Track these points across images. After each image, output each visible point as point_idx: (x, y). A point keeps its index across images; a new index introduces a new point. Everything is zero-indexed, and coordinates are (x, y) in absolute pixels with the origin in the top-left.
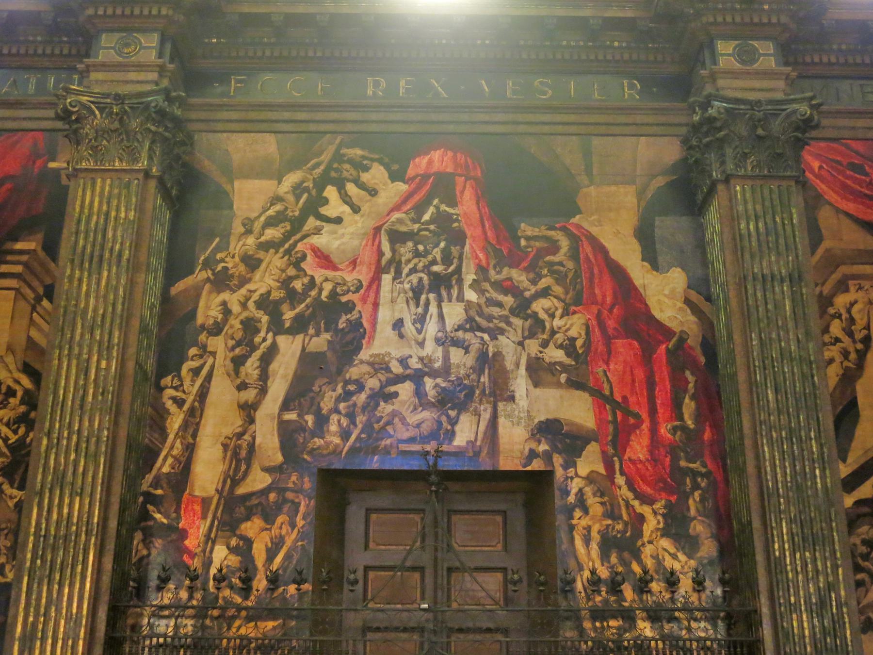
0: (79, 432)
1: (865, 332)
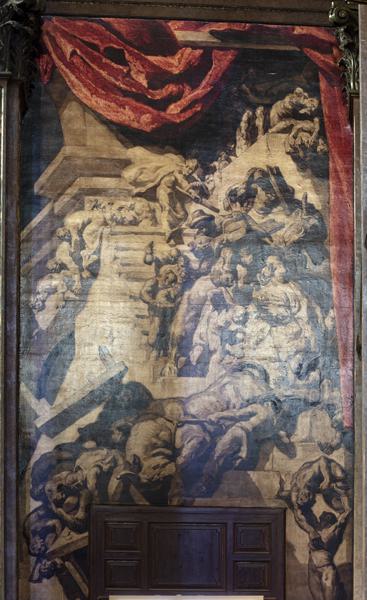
1: (95, 257)
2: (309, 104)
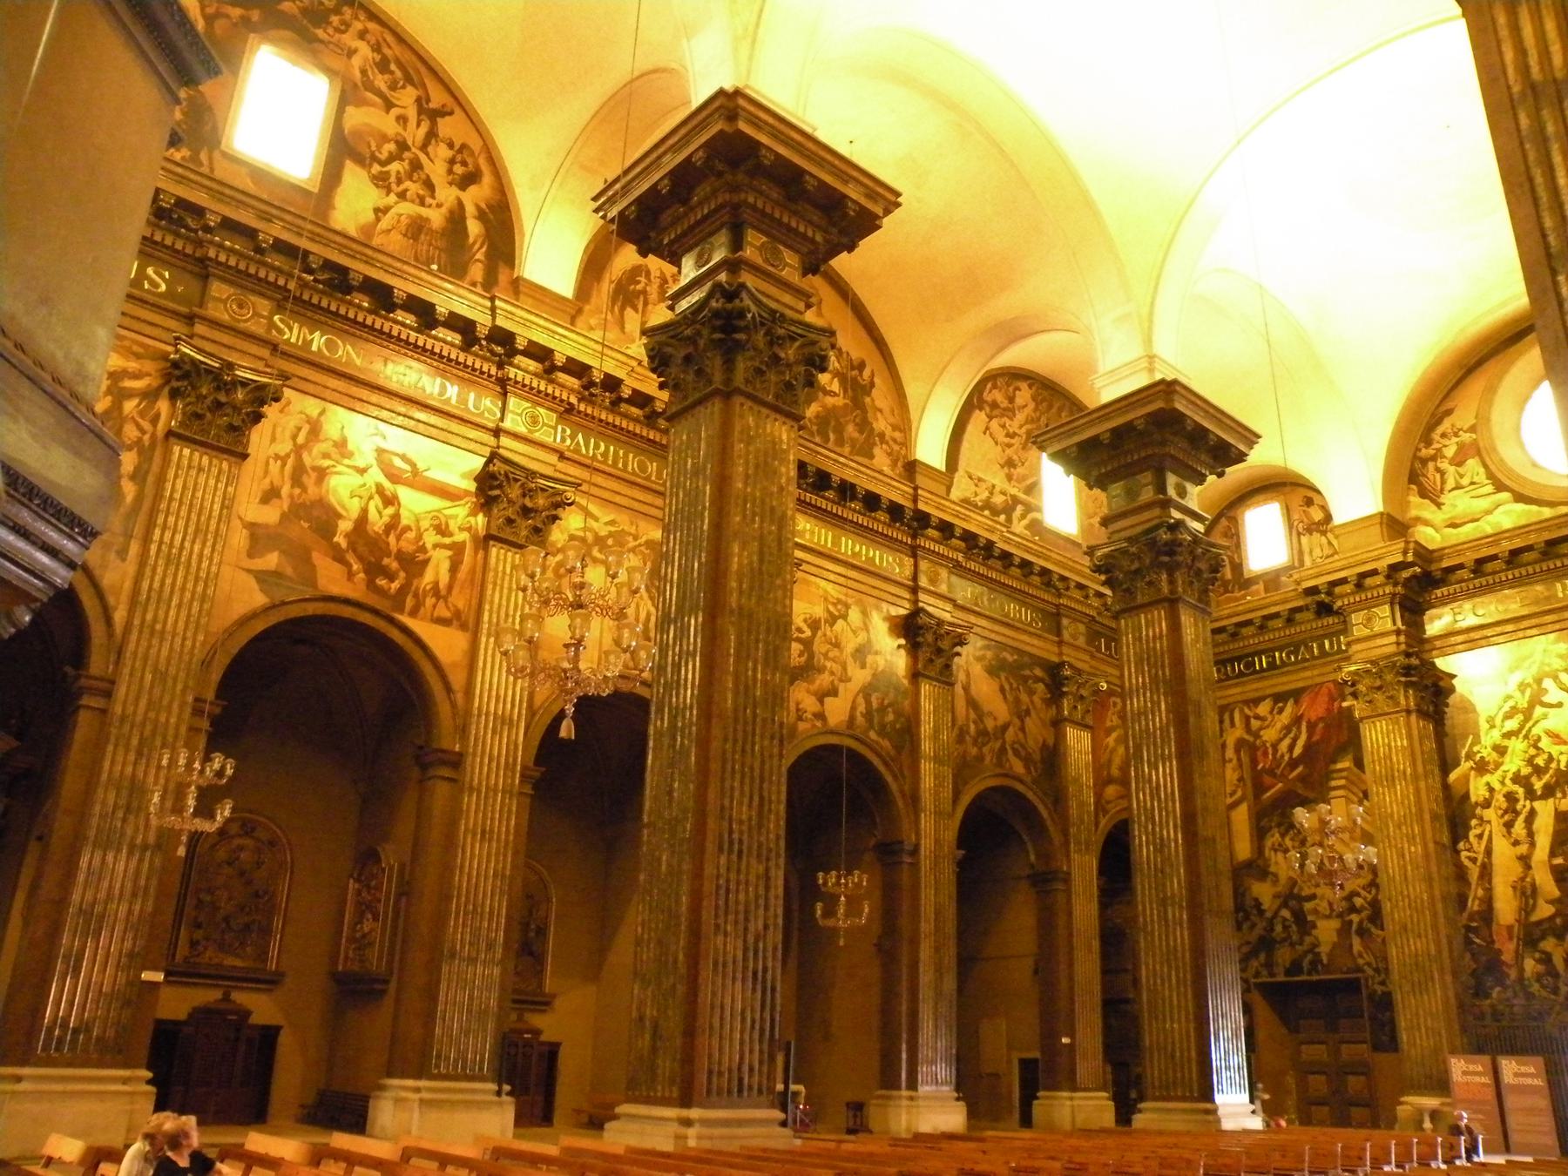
0: (1409, 896)
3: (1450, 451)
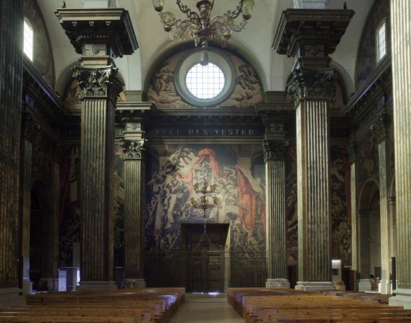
2: (341, 161)
3: (165, 77)
